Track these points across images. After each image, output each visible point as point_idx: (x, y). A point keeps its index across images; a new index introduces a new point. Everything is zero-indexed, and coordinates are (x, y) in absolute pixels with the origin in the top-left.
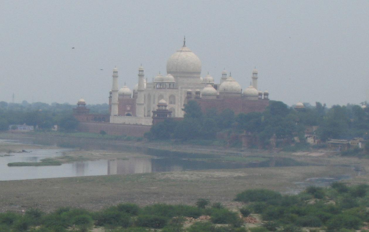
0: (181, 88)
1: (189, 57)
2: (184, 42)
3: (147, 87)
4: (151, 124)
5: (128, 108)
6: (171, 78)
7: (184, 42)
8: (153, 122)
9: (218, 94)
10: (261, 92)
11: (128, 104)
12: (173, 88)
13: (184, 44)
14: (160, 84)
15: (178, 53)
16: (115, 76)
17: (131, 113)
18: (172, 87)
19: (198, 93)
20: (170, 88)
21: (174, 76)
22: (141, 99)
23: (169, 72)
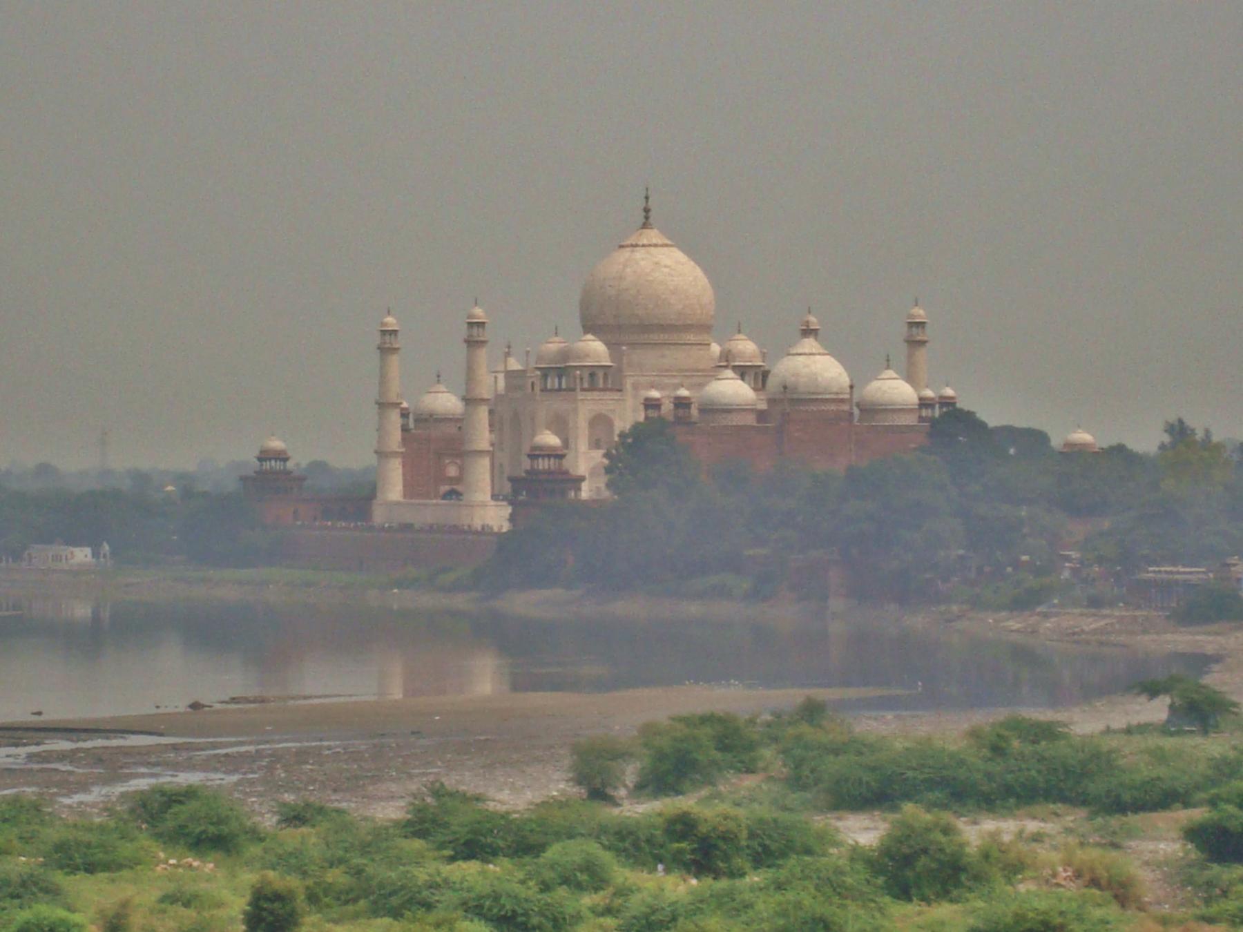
0: (636, 387)
1: (666, 269)
2: (647, 210)
3: (509, 387)
6: (595, 348)
7: (647, 210)
11: (433, 449)
12: (605, 390)
13: (647, 218)
14: (561, 372)
15: (626, 253)
16: (387, 344)
18: (601, 385)
20: (592, 388)
21: (608, 344)
22: (482, 437)
23: (591, 326)
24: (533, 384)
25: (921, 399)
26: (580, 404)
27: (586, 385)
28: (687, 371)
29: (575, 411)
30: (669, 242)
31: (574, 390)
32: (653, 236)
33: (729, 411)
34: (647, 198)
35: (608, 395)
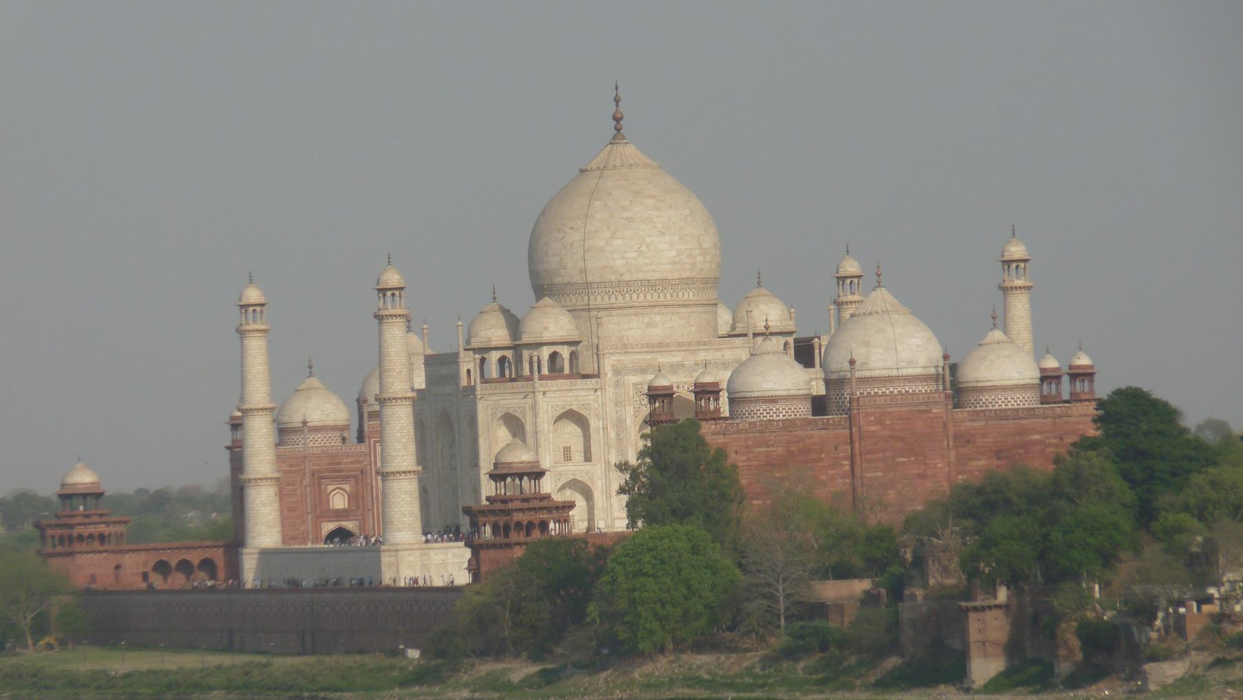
0: (617, 372)
2: (617, 119)
3: (429, 379)
4: (463, 578)
5: (339, 501)
7: (617, 119)
8: (474, 568)
9: (819, 389)
10: (1051, 363)
17: (350, 525)
19: (705, 391)
24: (469, 371)
25: (1042, 370)
26: (540, 396)
27: (545, 371)
28: (689, 344)
29: (534, 407)
30: (649, 161)
31: (530, 379)
32: (628, 151)
33: (773, 400)
34: (617, 101)
35: (580, 383)
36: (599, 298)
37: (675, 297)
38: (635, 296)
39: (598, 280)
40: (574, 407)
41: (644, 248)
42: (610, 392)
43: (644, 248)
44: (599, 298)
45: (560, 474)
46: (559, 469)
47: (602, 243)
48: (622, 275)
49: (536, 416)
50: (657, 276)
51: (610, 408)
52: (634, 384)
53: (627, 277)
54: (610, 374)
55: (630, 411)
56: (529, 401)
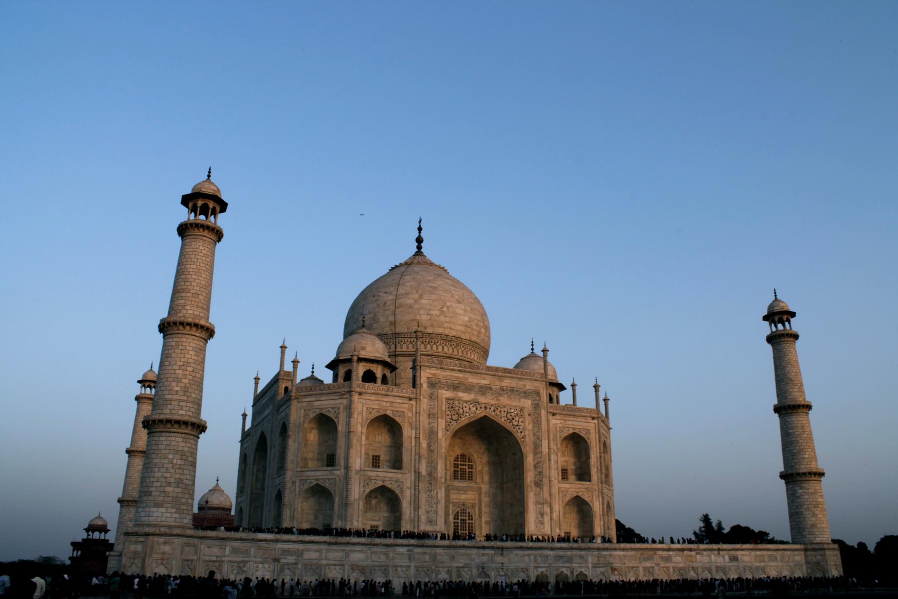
36: (404, 346)
37: (465, 354)
38: (434, 348)
39: (405, 331)
40: (389, 413)
41: (445, 309)
42: (424, 403)
43: (445, 309)
44: (404, 346)
45: (370, 479)
46: (370, 474)
47: (410, 302)
48: (426, 328)
49: (350, 416)
50: (454, 333)
51: (424, 420)
52: (447, 399)
53: (429, 330)
54: (425, 386)
55: (442, 424)
56: (345, 401)
